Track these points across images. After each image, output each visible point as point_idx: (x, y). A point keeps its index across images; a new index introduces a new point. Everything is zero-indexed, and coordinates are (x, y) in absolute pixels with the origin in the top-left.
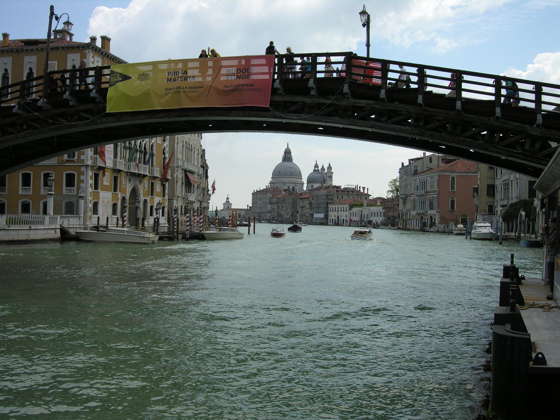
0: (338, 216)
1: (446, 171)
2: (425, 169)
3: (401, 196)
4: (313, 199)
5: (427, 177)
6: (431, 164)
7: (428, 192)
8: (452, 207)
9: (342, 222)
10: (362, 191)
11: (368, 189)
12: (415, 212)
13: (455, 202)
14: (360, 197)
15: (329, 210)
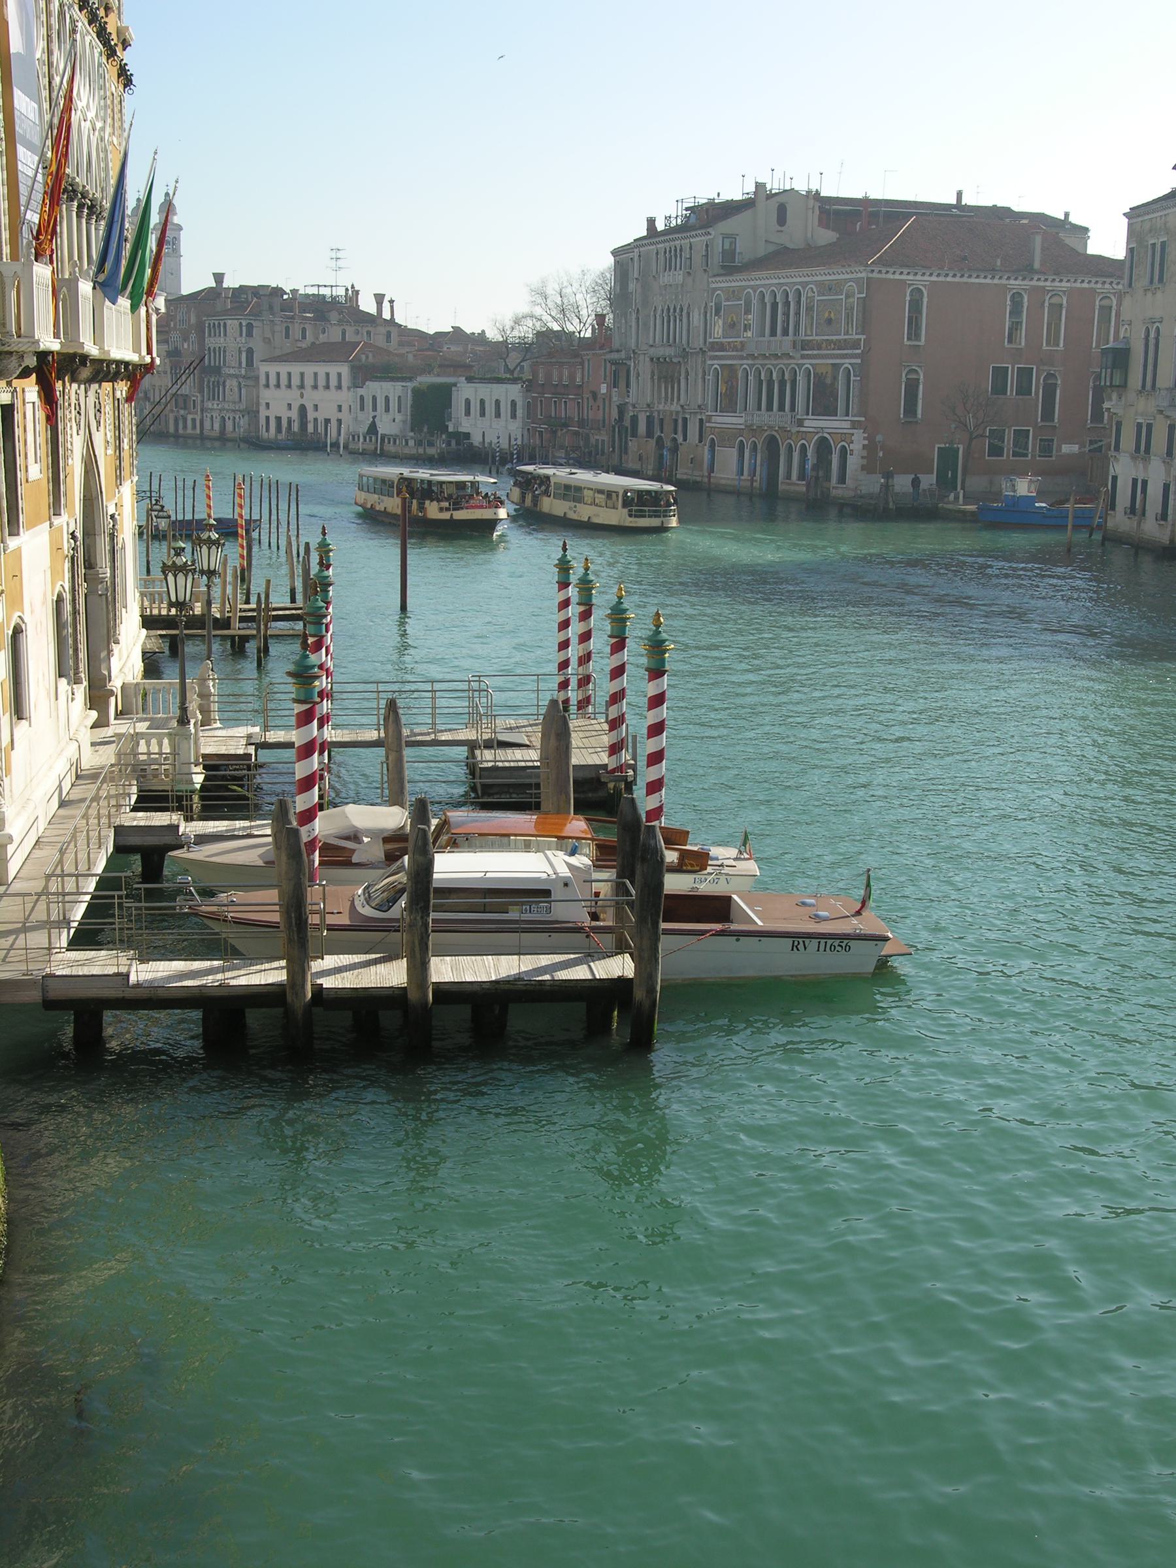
0: (303, 409)
1: (891, 266)
2: (761, 251)
3: (652, 351)
4: (186, 339)
5: (807, 283)
6: (782, 228)
7: (805, 345)
8: (910, 409)
9: (321, 429)
10: (367, 305)
11: (391, 302)
12: (741, 421)
13: (921, 387)
14: (369, 333)
15: (263, 381)
